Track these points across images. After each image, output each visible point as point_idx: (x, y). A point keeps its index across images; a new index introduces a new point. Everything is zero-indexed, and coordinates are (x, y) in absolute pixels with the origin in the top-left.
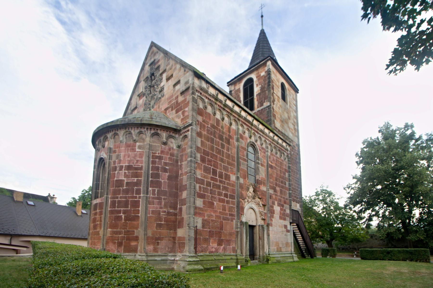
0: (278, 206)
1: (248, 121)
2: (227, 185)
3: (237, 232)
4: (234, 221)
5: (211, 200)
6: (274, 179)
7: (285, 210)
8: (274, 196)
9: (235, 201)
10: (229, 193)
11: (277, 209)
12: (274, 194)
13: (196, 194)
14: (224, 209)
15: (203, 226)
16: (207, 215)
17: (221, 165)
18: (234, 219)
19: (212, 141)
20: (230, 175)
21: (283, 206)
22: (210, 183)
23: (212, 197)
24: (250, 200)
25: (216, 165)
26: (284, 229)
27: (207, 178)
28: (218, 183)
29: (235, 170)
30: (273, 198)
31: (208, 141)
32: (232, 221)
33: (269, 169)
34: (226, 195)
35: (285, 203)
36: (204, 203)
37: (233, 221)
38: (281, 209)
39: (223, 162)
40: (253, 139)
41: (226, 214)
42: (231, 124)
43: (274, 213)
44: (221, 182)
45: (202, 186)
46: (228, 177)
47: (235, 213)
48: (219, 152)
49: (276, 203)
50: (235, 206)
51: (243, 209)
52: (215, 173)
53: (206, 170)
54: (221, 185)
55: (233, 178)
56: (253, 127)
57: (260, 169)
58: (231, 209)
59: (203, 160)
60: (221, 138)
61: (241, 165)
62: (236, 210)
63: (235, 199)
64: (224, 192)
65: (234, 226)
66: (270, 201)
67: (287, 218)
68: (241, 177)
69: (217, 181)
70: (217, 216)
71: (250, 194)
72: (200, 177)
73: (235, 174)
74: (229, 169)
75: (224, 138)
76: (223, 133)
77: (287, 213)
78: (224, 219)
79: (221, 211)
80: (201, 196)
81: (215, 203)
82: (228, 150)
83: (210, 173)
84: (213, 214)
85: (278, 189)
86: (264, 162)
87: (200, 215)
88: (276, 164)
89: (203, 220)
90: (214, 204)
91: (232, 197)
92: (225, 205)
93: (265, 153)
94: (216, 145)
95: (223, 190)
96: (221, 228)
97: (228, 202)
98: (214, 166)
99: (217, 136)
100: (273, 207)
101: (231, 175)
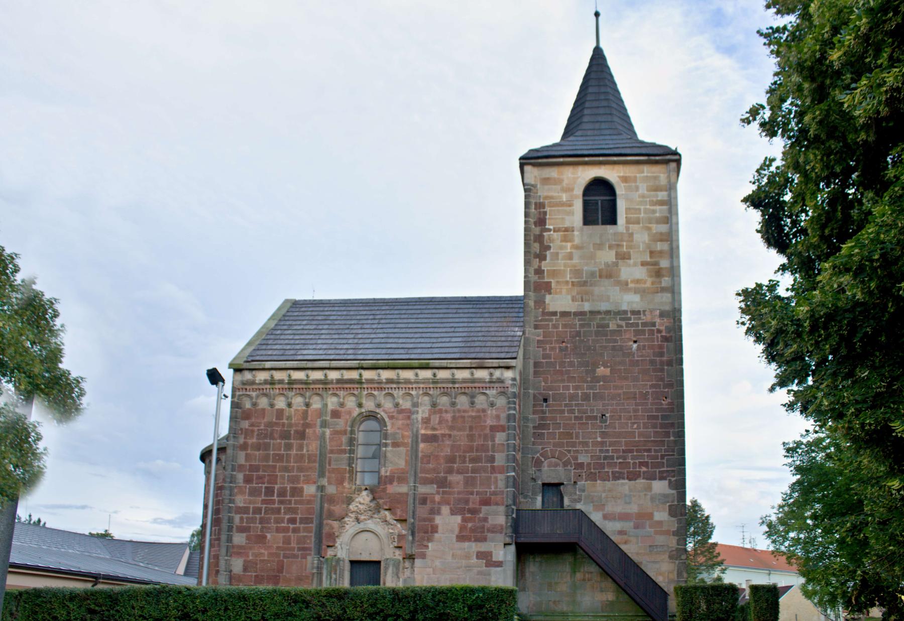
0: (453, 513)
1: (351, 381)
2: (295, 504)
3: (313, 574)
4: (309, 558)
5: (262, 531)
6: (442, 461)
7: (485, 519)
8: (437, 498)
9: (313, 526)
10: (298, 516)
11: (448, 522)
12: (438, 493)
13: (234, 529)
14: (287, 541)
15: (245, 569)
16: (253, 554)
17: (283, 477)
18: (310, 554)
19: (266, 447)
20: (302, 488)
21: (474, 512)
22: (260, 509)
23: (263, 527)
24: (362, 517)
25: (273, 479)
26: (474, 560)
27: (254, 503)
28: (276, 505)
29: (314, 475)
30: (433, 501)
31: (259, 450)
32: (304, 557)
33: (422, 446)
34: (292, 521)
35: (486, 502)
36: (248, 538)
37: (306, 558)
38: (464, 520)
39: (289, 471)
40: (369, 405)
41: (293, 549)
42: (308, 405)
43: (437, 532)
44: (281, 502)
45: (245, 516)
46: (298, 492)
47: (312, 545)
48: (280, 458)
49: (445, 510)
50: (313, 534)
51: (332, 537)
52: (269, 491)
53: (254, 492)
54: (282, 507)
55: (310, 490)
56: (365, 386)
57: (389, 455)
58: (300, 541)
59: (248, 480)
60: (285, 435)
61: (333, 463)
62: (313, 539)
63: (312, 523)
64: (287, 517)
65: (309, 566)
66: (422, 511)
67: (490, 535)
68: (330, 483)
69: (274, 503)
70: (270, 554)
71: (361, 507)
72: (241, 505)
73: (315, 483)
74: (302, 478)
75: (292, 432)
76: (290, 425)
77: (495, 526)
78: (285, 556)
79: (281, 545)
80: (241, 530)
81: (269, 536)
82: (301, 448)
83: (260, 495)
84: (263, 551)
85: (455, 478)
86: (403, 436)
87: (239, 554)
88: (452, 428)
89: (245, 561)
90: (266, 537)
91: (305, 520)
92: (290, 537)
93: (409, 418)
94: (274, 450)
95: (285, 513)
96: (280, 569)
97: (295, 530)
98: (268, 483)
99: (276, 435)
100: (432, 520)
101: (305, 487)
